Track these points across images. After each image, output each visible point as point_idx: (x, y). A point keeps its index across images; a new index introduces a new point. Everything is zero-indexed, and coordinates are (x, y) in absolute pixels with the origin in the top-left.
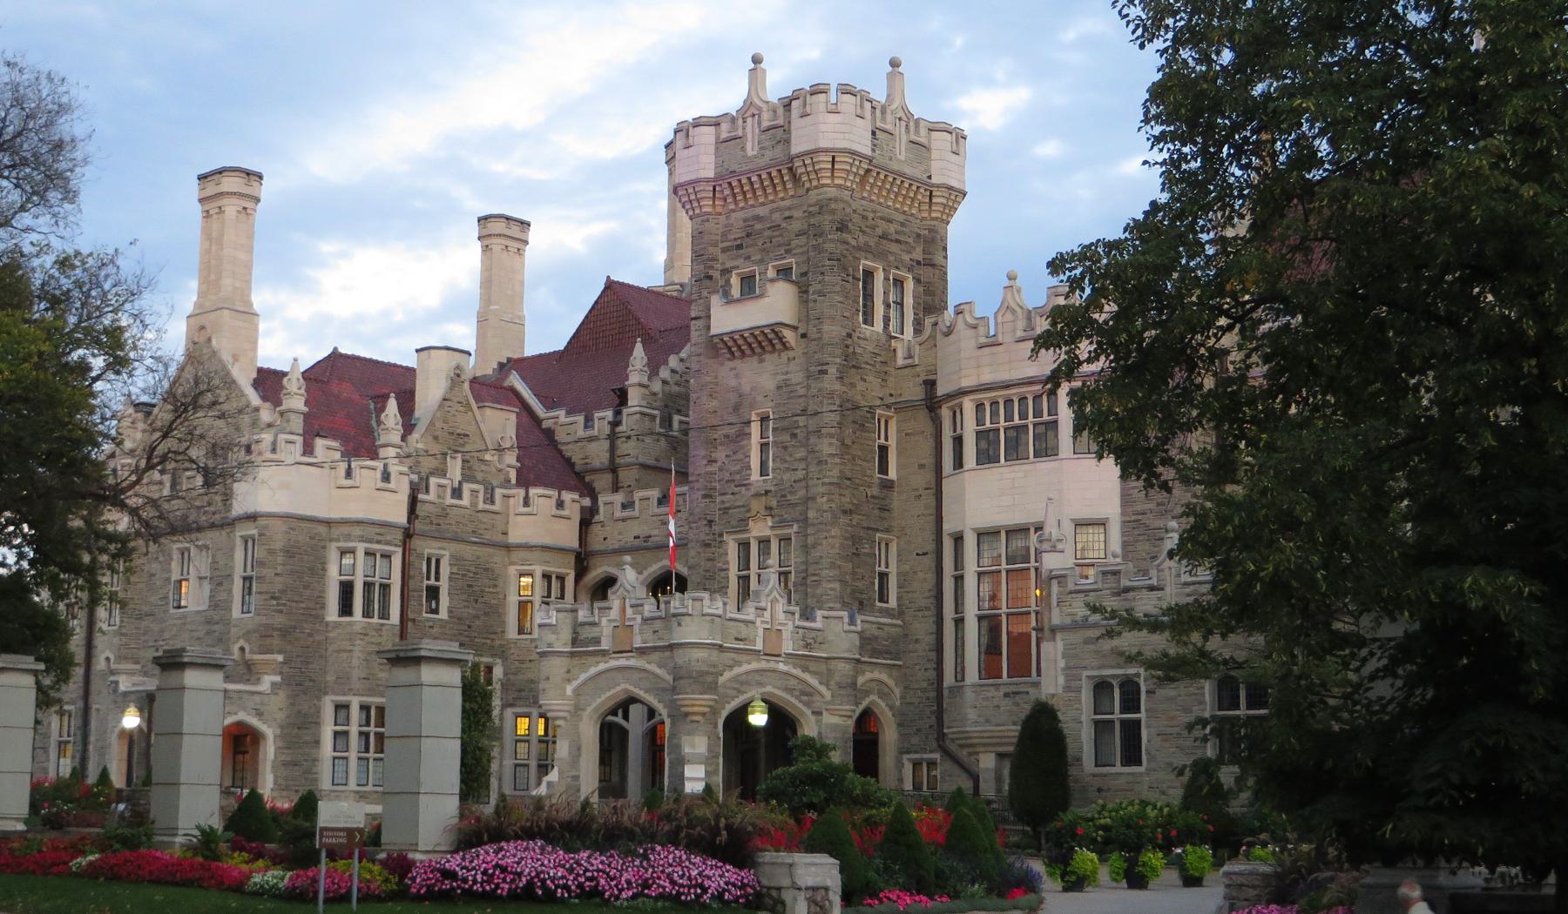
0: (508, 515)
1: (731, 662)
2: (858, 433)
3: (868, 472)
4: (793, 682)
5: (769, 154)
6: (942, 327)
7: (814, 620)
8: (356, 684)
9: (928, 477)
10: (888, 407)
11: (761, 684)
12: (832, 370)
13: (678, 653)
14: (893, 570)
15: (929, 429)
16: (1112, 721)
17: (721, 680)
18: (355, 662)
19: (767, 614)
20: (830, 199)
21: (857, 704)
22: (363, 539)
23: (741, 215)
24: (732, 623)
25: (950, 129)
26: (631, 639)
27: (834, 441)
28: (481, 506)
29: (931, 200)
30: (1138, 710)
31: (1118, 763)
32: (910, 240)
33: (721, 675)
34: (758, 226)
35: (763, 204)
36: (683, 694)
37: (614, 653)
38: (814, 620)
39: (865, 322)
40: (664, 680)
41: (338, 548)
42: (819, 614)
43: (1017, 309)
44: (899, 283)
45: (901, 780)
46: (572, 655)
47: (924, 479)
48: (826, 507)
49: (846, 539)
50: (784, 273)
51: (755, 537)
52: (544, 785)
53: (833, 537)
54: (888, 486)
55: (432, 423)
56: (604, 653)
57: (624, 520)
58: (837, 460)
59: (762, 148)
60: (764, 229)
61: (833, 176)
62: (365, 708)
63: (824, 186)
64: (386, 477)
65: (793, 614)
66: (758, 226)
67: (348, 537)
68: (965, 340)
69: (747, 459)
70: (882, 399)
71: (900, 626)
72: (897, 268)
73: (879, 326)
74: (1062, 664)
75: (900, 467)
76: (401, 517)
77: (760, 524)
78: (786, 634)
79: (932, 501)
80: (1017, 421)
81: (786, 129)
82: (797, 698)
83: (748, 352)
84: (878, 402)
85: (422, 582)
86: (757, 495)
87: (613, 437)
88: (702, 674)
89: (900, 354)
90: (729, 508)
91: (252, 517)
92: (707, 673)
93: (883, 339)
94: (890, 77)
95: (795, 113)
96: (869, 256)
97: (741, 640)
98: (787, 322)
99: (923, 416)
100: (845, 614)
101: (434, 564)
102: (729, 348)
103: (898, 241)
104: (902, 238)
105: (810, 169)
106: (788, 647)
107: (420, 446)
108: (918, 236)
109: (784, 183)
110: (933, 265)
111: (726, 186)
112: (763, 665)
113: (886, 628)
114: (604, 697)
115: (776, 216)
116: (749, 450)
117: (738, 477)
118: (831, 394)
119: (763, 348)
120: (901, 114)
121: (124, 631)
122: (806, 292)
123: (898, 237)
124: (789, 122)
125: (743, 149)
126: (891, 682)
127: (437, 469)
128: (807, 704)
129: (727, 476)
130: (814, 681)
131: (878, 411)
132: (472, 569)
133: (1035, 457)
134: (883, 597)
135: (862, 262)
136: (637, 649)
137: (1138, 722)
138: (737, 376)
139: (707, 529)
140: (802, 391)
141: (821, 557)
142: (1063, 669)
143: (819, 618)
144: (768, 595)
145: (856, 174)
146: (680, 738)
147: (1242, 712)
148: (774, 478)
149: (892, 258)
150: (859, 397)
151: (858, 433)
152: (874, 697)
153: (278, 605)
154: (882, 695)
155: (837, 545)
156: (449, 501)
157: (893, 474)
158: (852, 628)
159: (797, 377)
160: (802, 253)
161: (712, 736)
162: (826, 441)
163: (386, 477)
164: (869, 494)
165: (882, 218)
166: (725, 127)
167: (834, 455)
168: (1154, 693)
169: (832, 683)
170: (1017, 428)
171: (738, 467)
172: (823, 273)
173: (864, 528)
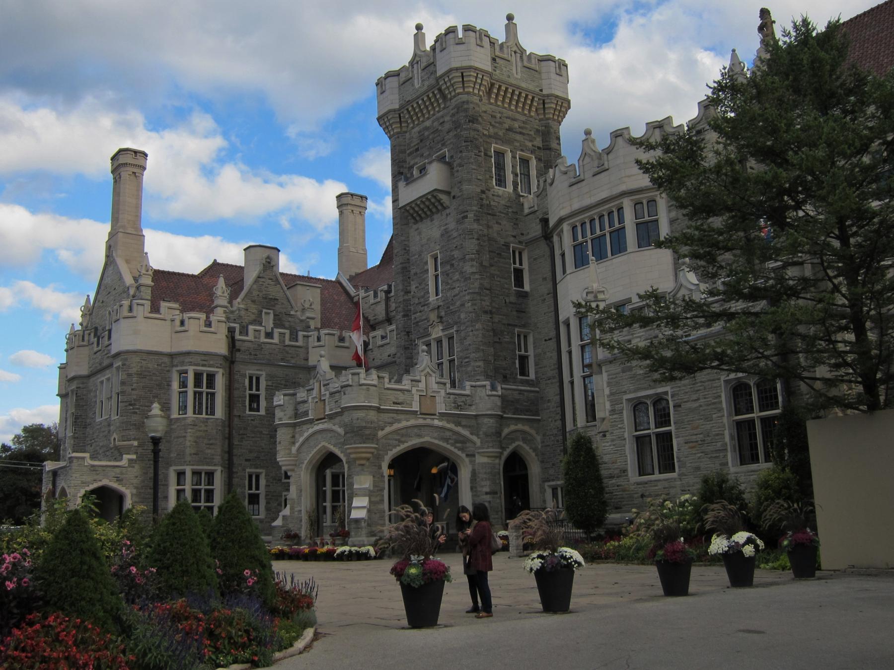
0: (307, 348)
1: (390, 420)
2: (496, 259)
3: (506, 286)
4: (448, 434)
5: (427, 83)
6: (549, 181)
7: (463, 388)
8: (188, 458)
9: (550, 285)
10: (520, 242)
11: (420, 436)
12: (471, 215)
14: (531, 353)
15: (547, 250)
16: (649, 436)
17: (381, 434)
18: (188, 444)
19: (422, 385)
20: (464, 102)
21: (503, 449)
22: (191, 364)
23: (417, 129)
24: (390, 392)
25: (552, 59)
26: (324, 408)
27: (475, 263)
28: (287, 342)
29: (544, 105)
30: (670, 425)
31: (656, 470)
32: (532, 133)
33: (382, 429)
34: (426, 133)
35: (428, 118)
36: (349, 444)
38: (463, 388)
39: (500, 185)
41: (178, 371)
42: (468, 384)
43: (593, 154)
44: (525, 162)
45: (544, 501)
46: (294, 426)
47: (547, 287)
48: (471, 309)
49: (488, 331)
50: (442, 159)
51: (434, 339)
52: (280, 518)
53: (477, 330)
54: (525, 295)
55: (250, 292)
56: (311, 422)
57: (382, 346)
58: (477, 276)
59: (423, 81)
60: (429, 135)
61: (464, 87)
62: (196, 473)
63: (459, 94)
64: (208, 324)
65: (445, 384)
66: (426, 133)
67: (182, 363)
68: (561, 184)
70: (515, 237)
71: (538, 392)
72: (522, 150)
73: (510, 189)
74: (607, 391)
75: (532, 282)
76: (221, 347)
77: (436, 329)
78: (439, 399)
79: (552, 302)
80: (598, 232)
81: (433, 64)
82: (452, 445)
83: (423, 215)
84: (512, 239)
85: (245, 392)
86: (433, 310)
87: (387, 299)
88: (362, 428)
89: (526, 206)
90: (418, 322)
91: (118, 355)
92: (365, 427)
93: (513, 196)
94: (507, 26)
95: (437, 50)
96: (499, 142)
97: (398, 404)
98: (440, 188)
99: (543, 244)
100: (487, 383)
101: (255, 381)
102: (412, 215)
103: (521, 133)
104: (524, 131)
105: (448, 84)
106: (441, 408)
107: (242, 306)
108: (538, 131)
109: (437, 100)
110: (550, 149)
111: (405, 112)
112: (421, 421)
113: (525, 393)
114: (313, 453)
115: (436, 124)
116: (428, 282)
118: (471, 232)
119: (430, 210)
120: (515, 49)
121: (76, 435)
122: (453, 168)
123: (521, 130)
125: (413, 85)
126: (533, 432)
127: (255, 320)
128: (462, 449)
129: (416, 301)
130: (466, 432)
131: (511, 245)
132: (283, 382)
133: (612, 255)
134: (524, 371)
135: (493, 145)
136: (327, 415)
137: (669, 435)
139: (406, 337)
141: (470, 344)
142: (608, 396)
143: (468, 387)
144: (422, 371)
145: (481, 85)
147: (756, 414)
148: (442, 296)
149: (518, 144)
150: (495, 235)
151: (496, 259)
152: (517, 443)
153: (133, 409)
154: (525, 440)
155: (480, 335)
156: (263, 339)
157: (527, 287)
158: (494, 393)
159: (452, 225)
160: (451, 143)
161: (378, 476)
162: (470, 263)
163: (208, 324)
164: (507, 301)
165: (507, 118)
166: (403, 75)
167: (473, 273)
168: (680, 406)
169: (481, 433)
170: (599, 237)
171: (422, 294)
172: (461, 152)
173: (504, 324)
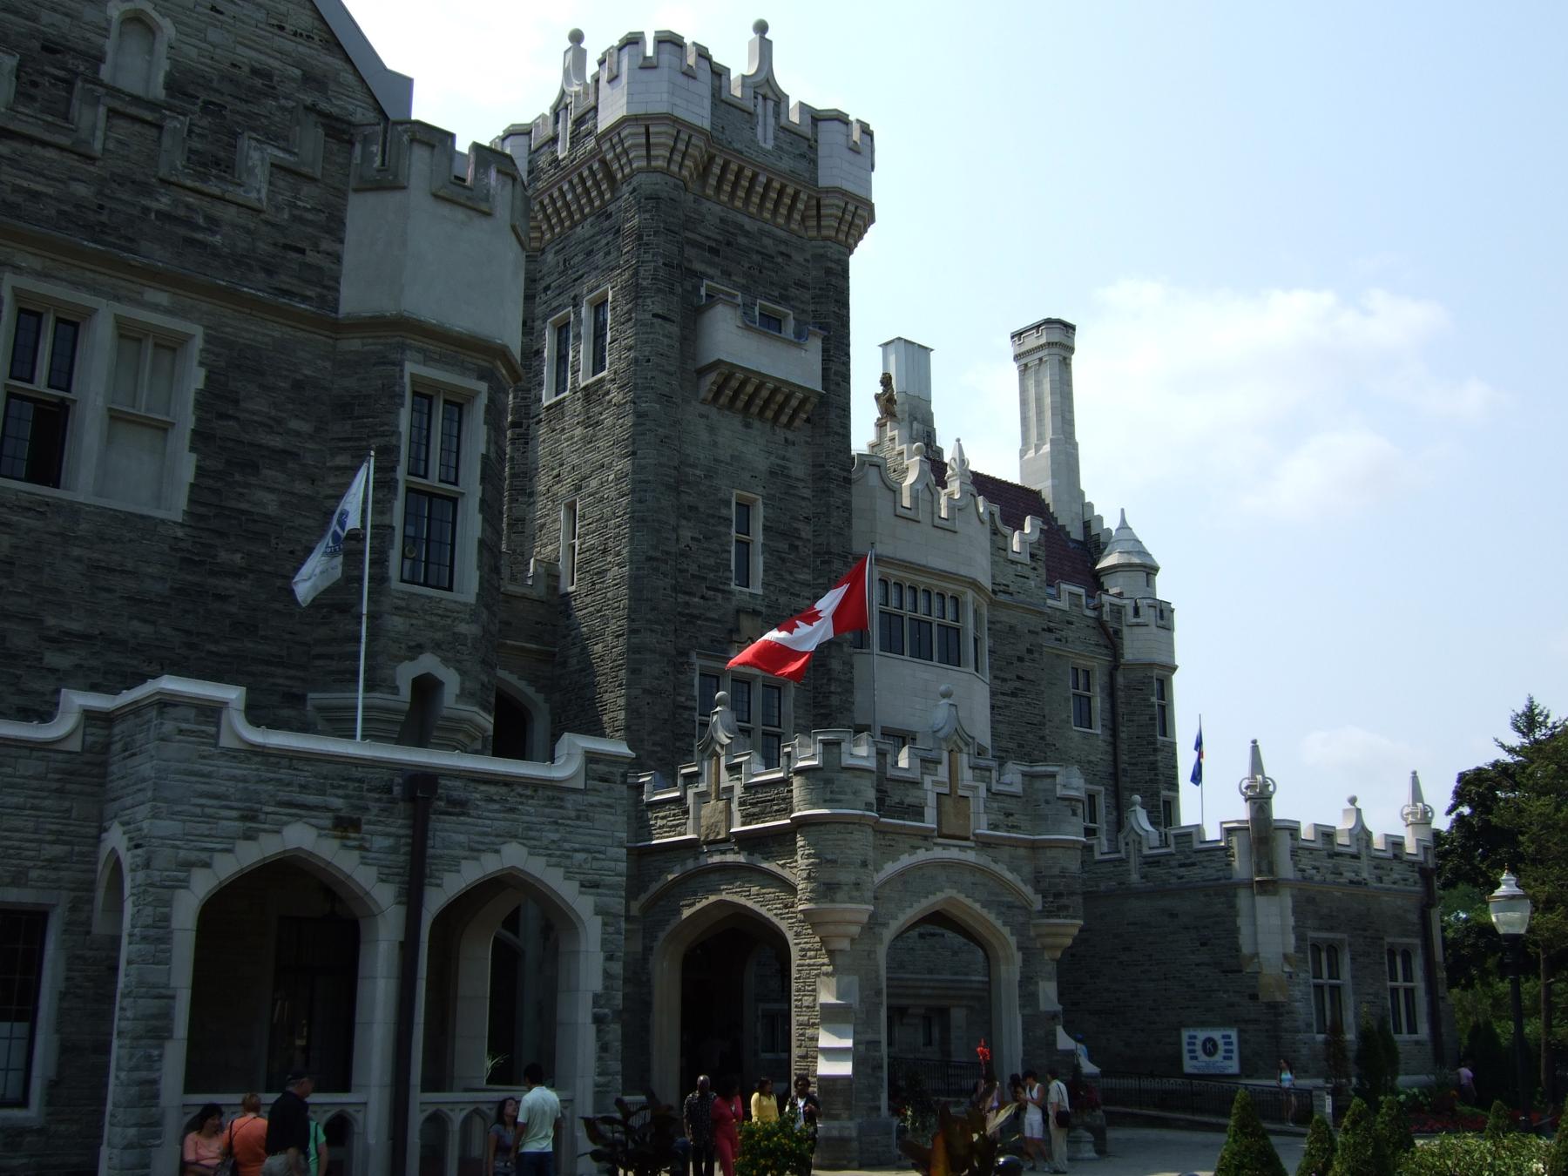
5: (786, 164)
13: (1050, 853)
34: (743, 241)
35: (750, 216)
37: (939, 836)
40: (1019, 893)
66: (743, 241)
69: (725, 555)
83: (740, 404)
90: (698, 617)
117: (711, 575)
124: (816, 141)
129: (693, 569)
138: (712, 429)
140: (807, 493)
146: (1037, 983)
148: (765, 596)
171: (711, 561)
